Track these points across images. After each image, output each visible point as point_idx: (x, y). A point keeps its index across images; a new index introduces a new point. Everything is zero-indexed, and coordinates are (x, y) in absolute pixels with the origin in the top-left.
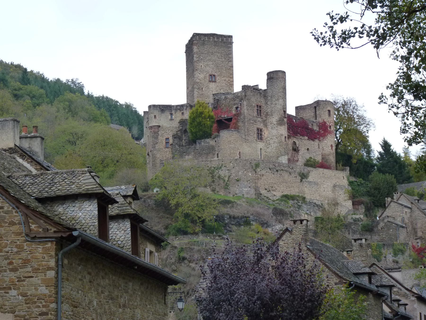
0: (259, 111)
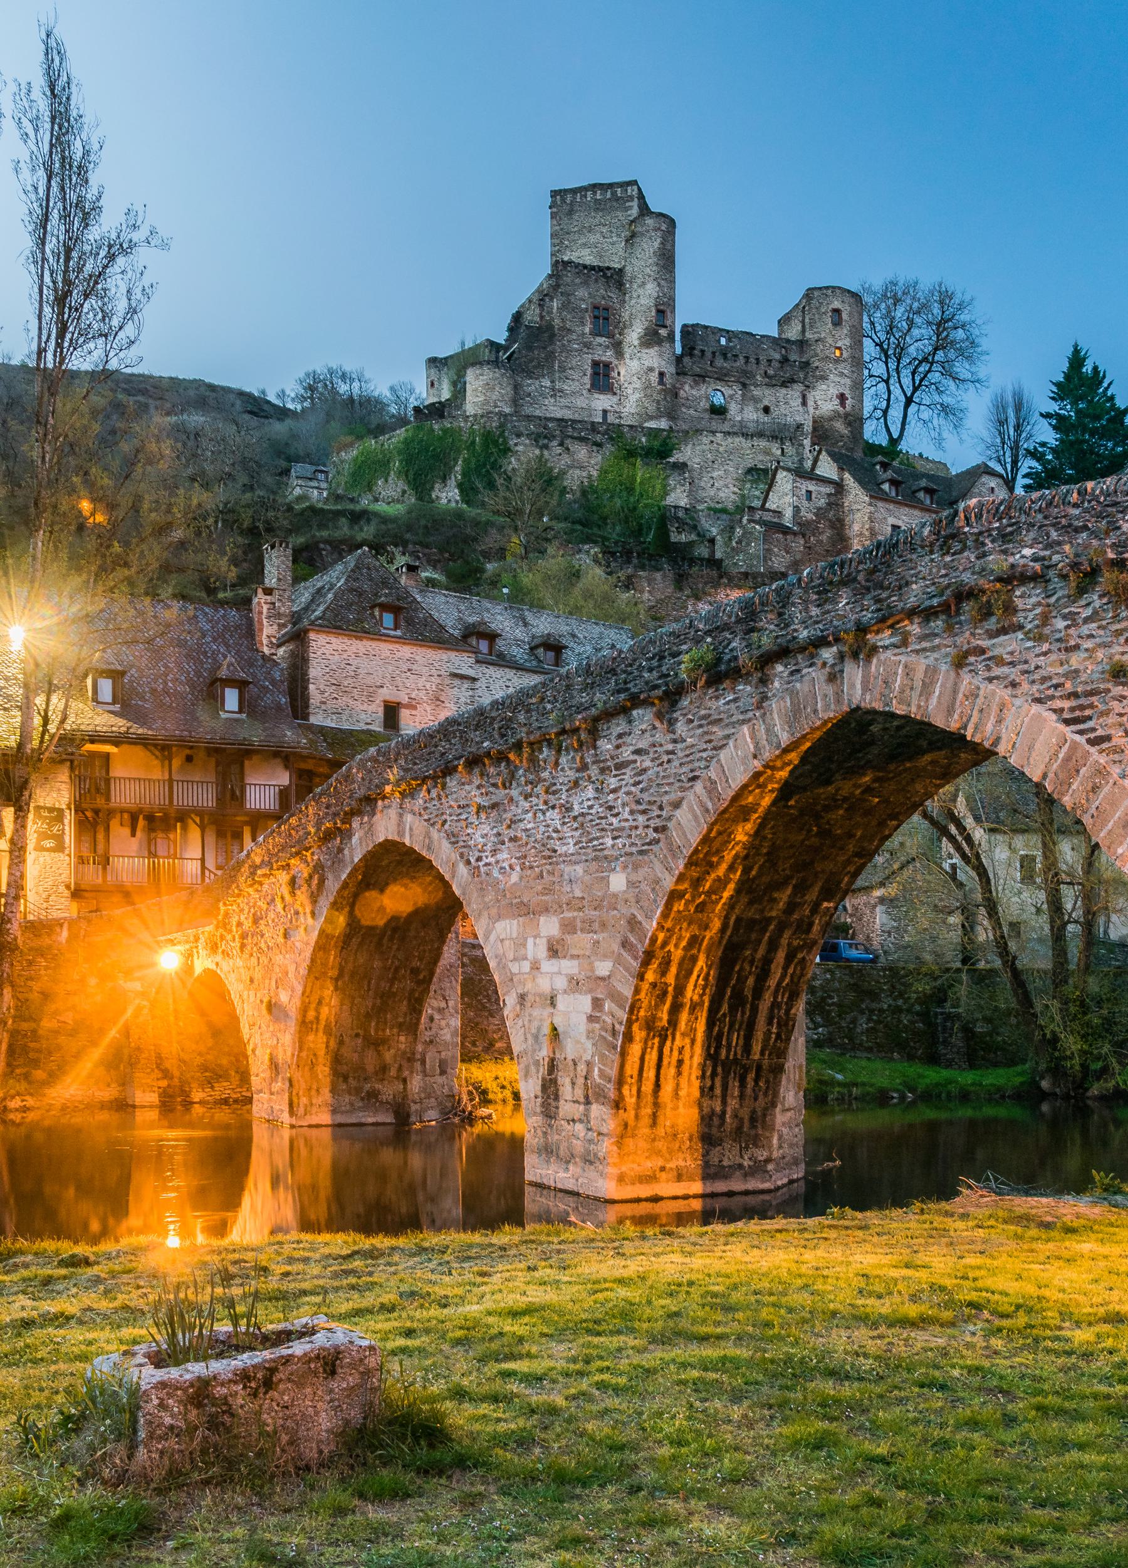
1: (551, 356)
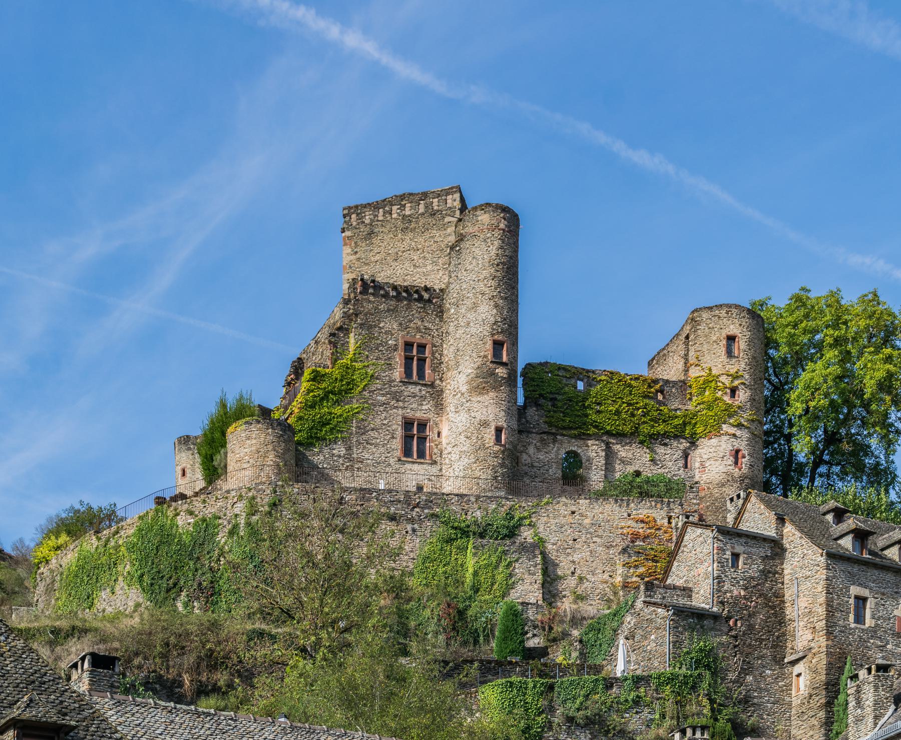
0: (415, 362)
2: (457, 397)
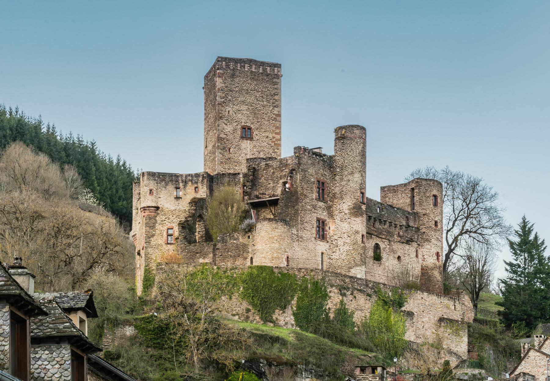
1: (296, 213)
2: (342, 214)
